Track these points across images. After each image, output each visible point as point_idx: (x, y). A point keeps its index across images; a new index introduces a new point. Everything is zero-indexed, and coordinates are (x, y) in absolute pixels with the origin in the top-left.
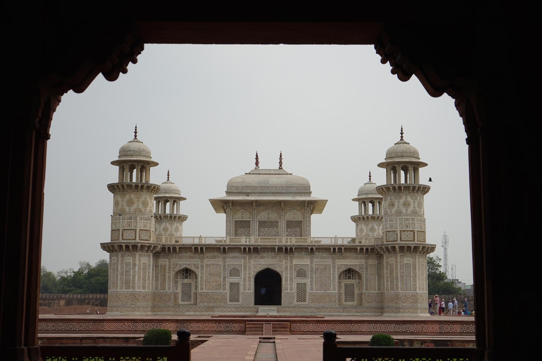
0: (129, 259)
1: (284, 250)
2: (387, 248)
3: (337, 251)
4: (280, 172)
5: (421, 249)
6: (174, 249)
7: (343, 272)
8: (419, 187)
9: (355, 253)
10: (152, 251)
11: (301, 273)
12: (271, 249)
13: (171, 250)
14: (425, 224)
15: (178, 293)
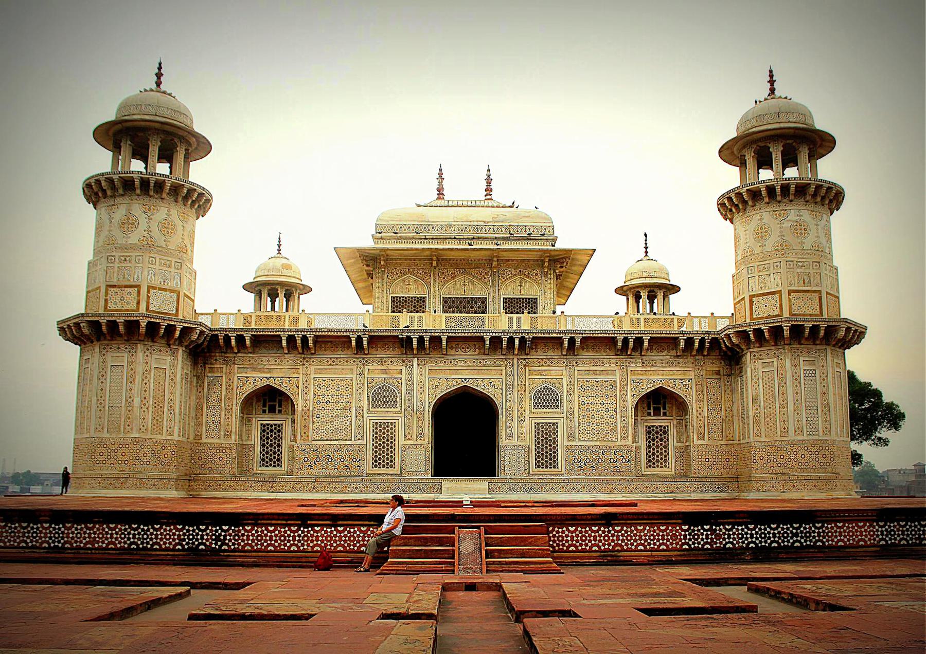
0: (119, 358)
1: (505, 343)
2: (759, 332)
3: (631, 344)
4: (490, 203)
5: (842, 333)
6: (240, 339)
7: (642, 400)
8: (829, 189)
9: (673, 353)
10: (180, 340)
11: (546, 398)
12: (474, 341)
13: (233, 342)
14: (837, 280)
15: (252, 446)
